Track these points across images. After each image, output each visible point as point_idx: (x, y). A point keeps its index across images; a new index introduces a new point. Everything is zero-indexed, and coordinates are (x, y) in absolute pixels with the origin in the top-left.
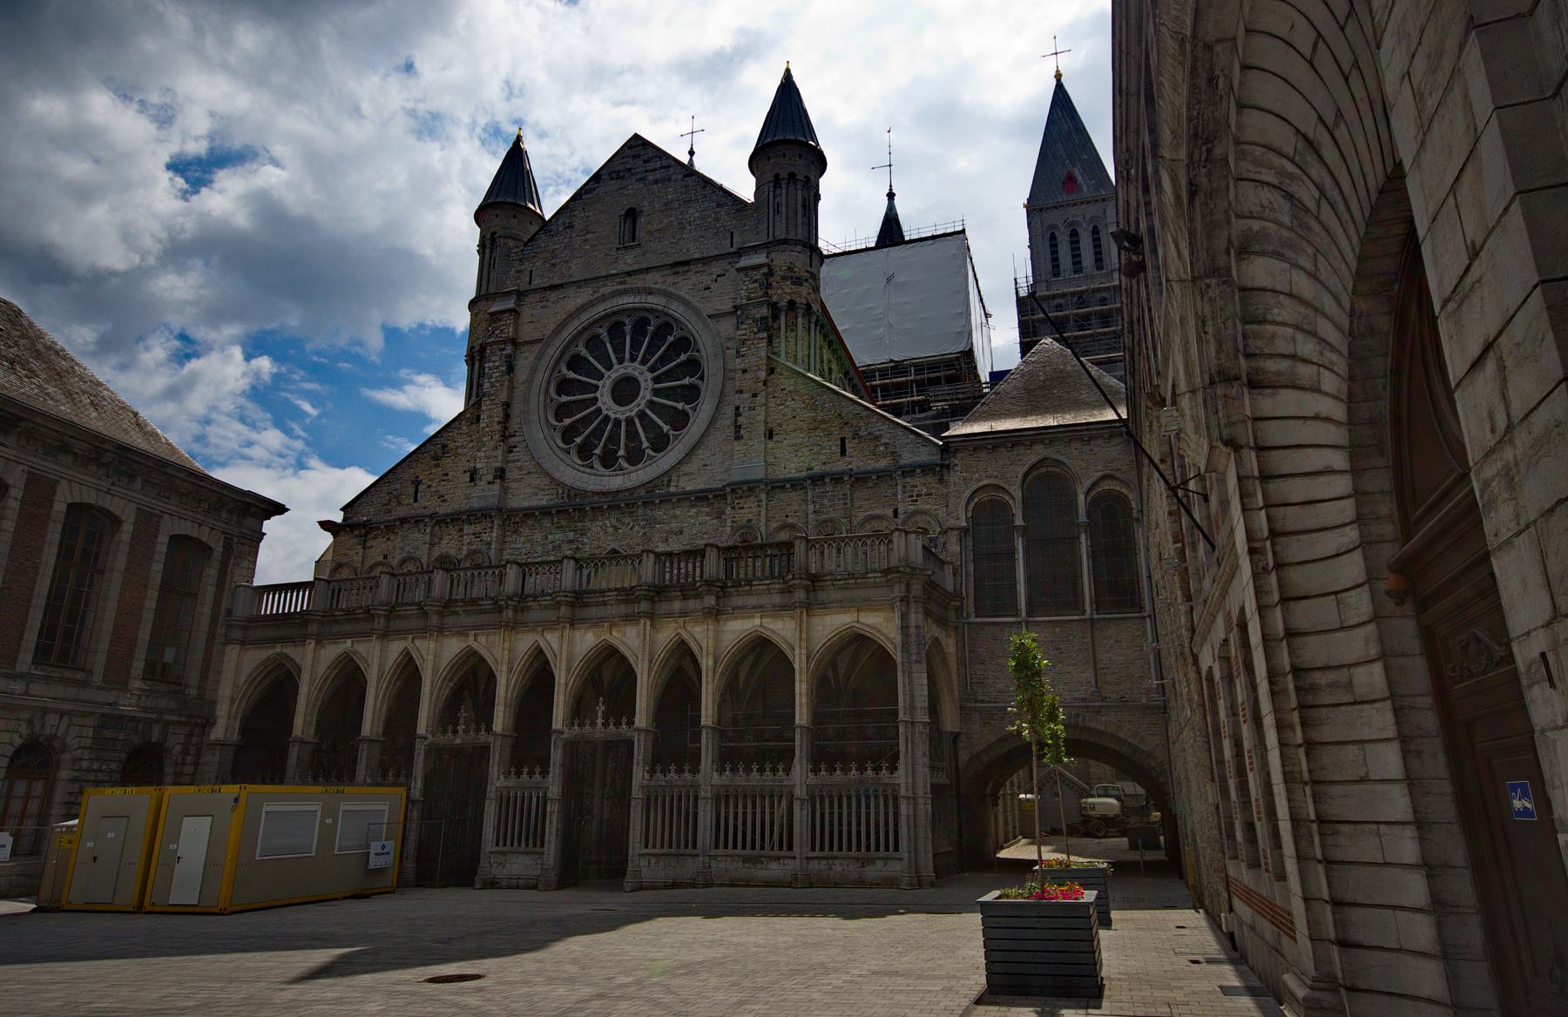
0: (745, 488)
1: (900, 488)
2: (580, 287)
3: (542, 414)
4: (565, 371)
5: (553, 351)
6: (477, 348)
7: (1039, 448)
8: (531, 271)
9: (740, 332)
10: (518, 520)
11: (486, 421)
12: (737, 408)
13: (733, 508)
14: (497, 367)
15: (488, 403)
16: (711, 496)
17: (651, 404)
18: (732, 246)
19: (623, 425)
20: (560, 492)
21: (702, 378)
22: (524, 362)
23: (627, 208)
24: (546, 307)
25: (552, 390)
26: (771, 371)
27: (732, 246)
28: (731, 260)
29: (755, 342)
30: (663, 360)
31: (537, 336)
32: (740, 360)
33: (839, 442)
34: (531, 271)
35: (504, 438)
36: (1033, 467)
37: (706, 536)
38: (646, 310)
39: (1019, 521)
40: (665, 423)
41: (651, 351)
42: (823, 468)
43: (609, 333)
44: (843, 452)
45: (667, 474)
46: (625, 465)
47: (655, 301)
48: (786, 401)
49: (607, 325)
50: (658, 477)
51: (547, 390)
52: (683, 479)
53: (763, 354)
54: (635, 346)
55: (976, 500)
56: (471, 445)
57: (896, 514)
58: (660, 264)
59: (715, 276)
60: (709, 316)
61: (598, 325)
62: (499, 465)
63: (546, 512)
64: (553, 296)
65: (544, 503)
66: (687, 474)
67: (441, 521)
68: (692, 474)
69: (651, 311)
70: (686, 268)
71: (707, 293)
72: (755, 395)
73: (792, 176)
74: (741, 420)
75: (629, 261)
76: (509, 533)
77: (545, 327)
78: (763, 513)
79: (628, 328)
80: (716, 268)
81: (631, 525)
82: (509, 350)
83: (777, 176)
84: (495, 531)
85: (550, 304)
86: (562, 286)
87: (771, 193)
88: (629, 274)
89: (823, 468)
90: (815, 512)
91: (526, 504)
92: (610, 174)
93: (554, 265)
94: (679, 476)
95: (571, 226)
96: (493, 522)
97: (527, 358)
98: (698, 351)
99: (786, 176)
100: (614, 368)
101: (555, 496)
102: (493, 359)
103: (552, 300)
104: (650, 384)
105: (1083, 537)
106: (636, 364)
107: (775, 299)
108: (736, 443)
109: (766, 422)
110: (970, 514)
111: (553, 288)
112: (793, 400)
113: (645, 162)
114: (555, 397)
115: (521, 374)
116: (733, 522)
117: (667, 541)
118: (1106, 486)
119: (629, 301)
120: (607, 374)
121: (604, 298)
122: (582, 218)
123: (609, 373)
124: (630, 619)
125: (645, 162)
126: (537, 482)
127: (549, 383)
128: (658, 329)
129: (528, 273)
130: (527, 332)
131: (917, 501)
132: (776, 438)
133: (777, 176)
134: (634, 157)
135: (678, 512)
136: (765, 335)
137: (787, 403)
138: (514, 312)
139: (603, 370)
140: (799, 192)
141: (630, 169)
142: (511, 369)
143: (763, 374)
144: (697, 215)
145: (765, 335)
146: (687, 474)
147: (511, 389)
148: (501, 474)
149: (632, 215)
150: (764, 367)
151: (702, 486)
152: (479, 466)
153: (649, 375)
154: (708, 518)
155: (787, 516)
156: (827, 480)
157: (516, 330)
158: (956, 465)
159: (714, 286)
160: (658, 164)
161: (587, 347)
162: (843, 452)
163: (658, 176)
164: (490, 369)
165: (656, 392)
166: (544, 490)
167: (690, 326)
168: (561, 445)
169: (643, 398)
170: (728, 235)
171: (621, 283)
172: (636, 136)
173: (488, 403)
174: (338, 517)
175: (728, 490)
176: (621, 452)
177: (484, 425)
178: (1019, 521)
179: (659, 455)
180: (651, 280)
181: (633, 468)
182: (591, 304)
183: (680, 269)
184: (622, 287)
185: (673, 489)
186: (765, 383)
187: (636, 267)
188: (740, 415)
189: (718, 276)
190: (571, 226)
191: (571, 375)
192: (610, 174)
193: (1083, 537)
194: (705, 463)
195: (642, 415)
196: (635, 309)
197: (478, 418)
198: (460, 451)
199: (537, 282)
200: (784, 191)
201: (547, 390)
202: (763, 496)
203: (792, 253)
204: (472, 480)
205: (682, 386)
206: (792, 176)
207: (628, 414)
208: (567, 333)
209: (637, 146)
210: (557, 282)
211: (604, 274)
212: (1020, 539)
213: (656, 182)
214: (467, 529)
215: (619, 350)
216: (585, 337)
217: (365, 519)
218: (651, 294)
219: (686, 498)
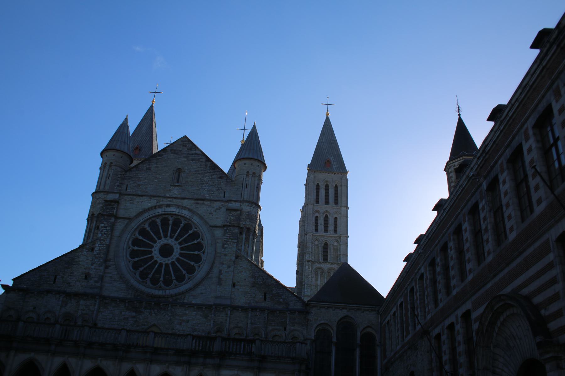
0: (222, 308)
1: (288, 319)
2: (151, 199)
3: (125, 254)
4: (137, 235)
5: (134, 225)
6: (96, 215)
7: (345, 311)
8: (127, 186)
9: (225, 237)
10: (107, 301)
11: (98, 252)
12: (220, 271)
13: (215, 315)
14: (106, 227)
15: (99, 243)
16: (204, 308)
17: (178, 260)
18: (224, 197)
19: (164, 266)
21: (204, 253)
22: (120, 226)
23: (178, 167)
25: (130, 243)
26: (237, 257)
27: (224, 197)
28: (223, 203)
29: (232, 243)
30: (186, 241)
31: (127, 216)
32: (223, 250)
33: (264, 294)
34: (127, 186)
35: (106, 260)
36: (342, 319)
37: (199, 325)
38: (181, 216)
39: (334, 340)
40: (184, 270)
41: (180, 235)
42: (256, 304)
43: (161, 222)
44: (265, 299)
45: (183, 293)
46: (163, 285)
47: (186, 213)
48: (242, 272)
49: (160, 218)
51: (128, 242)
53: (234, 249)
54: (174, 231)
55: (318, 329)
56: (87, 261)
57: (285, 329)
58: (190, 197)
59: (215, 209)
62: (101, 274)
63: (123, 300)
64: (137, 199)
65: (121, 296)
67: (70, 295)
69: (183, 217)
70: (202, 202)
72: (229, 267)
73: (254, 173)
74: (221, 276)
75: (176, 192)
76: (102, 307)
78: (228, 320)
79: (171, 222)
80: (217, 205)
81: (164, 314)
82: (113, 220)
83: (248, 172)
84: (97, 306)
86: (142, 196)
87: (244, 179)
88: (175, 198)
89: (256, 304)
90: (251, 323)
91: (112, 295)
92: (171, 150)
93: (139, 185)
95: (149, 169)
96: (96, 301)
98: (203, 240)
99: (252, 173)
102: (105, 222)
104: (179, 251)
105: (358, 350)
106: (173, 240)
107: (242, 226)
108: (218, 286)
109: (233, 280)
110: (315, 334)
111: (137, 195)
112: (245, 272)
113: (188, 149)
114: (131, 246)
115: (117, 233)
116: (214, 322)
117: (181, 324)
118: (369, 330)
119: (173, 210)
120: (158, 241)
121: (161, 206)
122: (156, 167)
123: (159, 241)
124: (178, 363)
125: (188, 149)
127: (129, 239)
128: (185, 225)
129: (125, 185)
130: (122, 213)
131: (295, 325)
132: (236, 287)
133: (248, 172)
134: (183, 146)
135: (187, 312)
136: (236, 241)
137: (243, 273)
138: (117, 202)
139: (156, 239)
140: (256, 181)
141: (181, 151)
142: (112, 230)
143: (233, 258)
144: (209, 179)
145: (236, 241)
147: (111, 239)
148: (101, 278)
149: (179, 171)
150: (234, 255)
151: (199, 302)
152: (91, 272)
153: (179, 247)
154: (201, 317)
155: (238, 323)
156: (258, 310)
157: (117, 211)
158: (312, 313)
160: (194, 152)
161: (149, 225)
162: (265, 299)
163: (194, 157)
164: (102, 227)
165: (181, 254)
168: (132, 270)
169: (175, 256)
170: (223, 192)
171: (171, 201)
172: (185, 137)
173: (99, 243)
174: (10, 284)
175: (214, 307)
176: (162, 279)
177: (95, 253)
178: (334, 340)
180: (186, 203)
181: (167, 288)
182: (155, 207)
183: (199, 202)
185: (185, 301)
186: (234, 262)
187: (179, 196)
188: (222, 275)
189: (217, 209)
190: (149, 169)
191: (141, 238)
192: (171, 150)
193: (358, 350)
195: (173, 263)
196: (175, 215)
197: (93, 249)
198: (80, 263)
199: (129, 191)
200: (250, 179)
201: (128, 242)
202: (229, 312)
203: (251, 208)
204: (86, 278)
205: (193, 254)
206: (254, 173)
207: (167, 262)
208: (142, 219)
209: (186, 141)
210: (140, 193)
211: (163, 195)
212: (334, 347)
213: (193, 160)
214: (82, 302)
215: (165, 231)
216: (149, 221)
217: (25, 287)
218: (184, 209)
219: (191, 305)
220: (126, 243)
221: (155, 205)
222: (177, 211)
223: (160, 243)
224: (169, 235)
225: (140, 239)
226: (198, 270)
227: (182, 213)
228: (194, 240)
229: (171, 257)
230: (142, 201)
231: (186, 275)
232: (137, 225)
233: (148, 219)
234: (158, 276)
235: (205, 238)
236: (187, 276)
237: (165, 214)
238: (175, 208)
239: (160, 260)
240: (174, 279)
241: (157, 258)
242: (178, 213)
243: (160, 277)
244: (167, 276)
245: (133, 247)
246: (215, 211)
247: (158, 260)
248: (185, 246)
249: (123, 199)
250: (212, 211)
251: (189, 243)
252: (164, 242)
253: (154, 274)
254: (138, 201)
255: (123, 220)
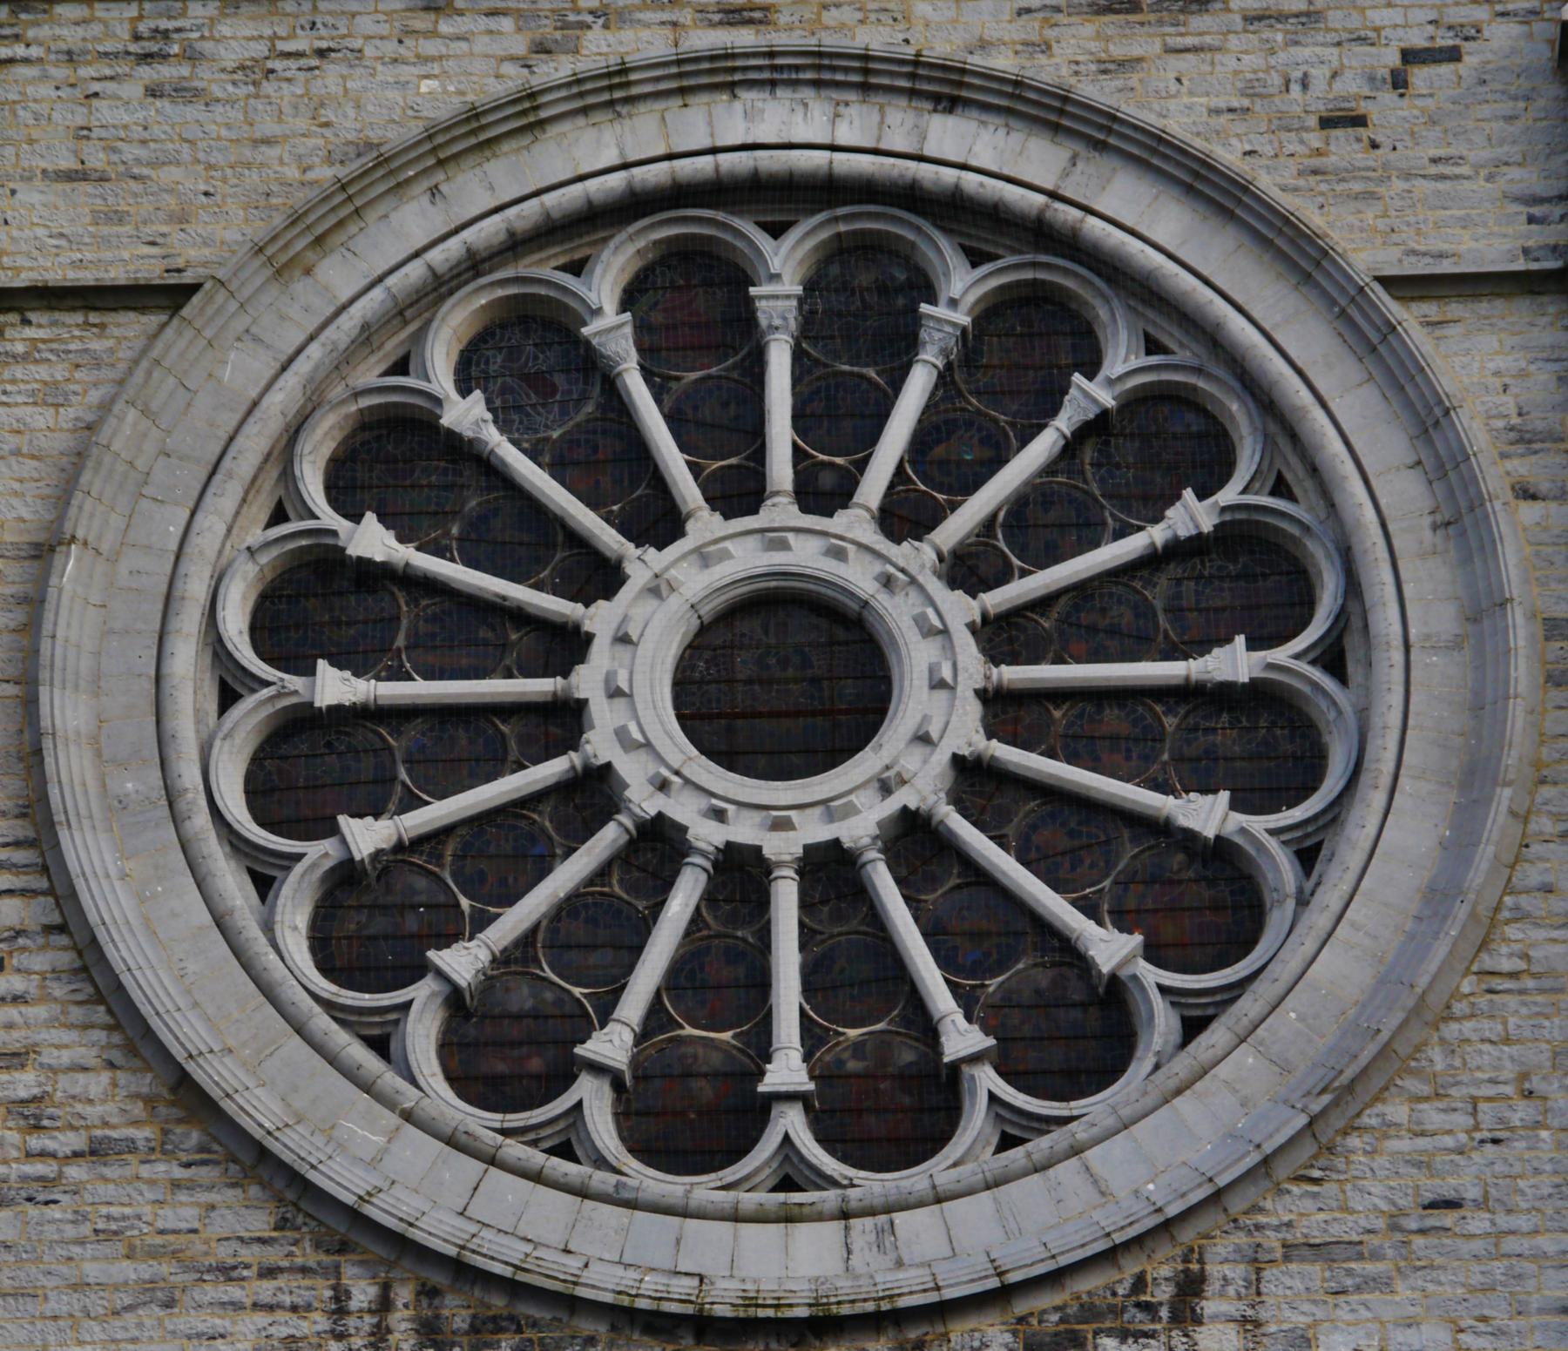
19: (786, 897)
20: (362, 1293)
21: (1332, 657)
24: (183, 92)
38: (911, 197)
50: (1110, 1256)
52: (1284, 1282)
59: (1392, 58)
60: (1386, 282)
61: (563, 252)
66: (1290, 1251)
68: (1356, 1250)
71: (1344, 147)
77: (181, 218)
85: (205, 76)
94: (1257, 1262)
97: (49, 395)
98: (1281, 488)
100: (840, 522)
101: (321, 1322)
103: (231, 55)
126: (183, 1213)
139: (608, 537)
146: (1317, 1250)
159: (1386, 110)
166: (227, 1272)
167: (1237, 326)
179: (1095, 1108)
184: (744, 38)
189: (1410, 56)
194: (1434, 1187)
218: (949, 103)
220: (189, 621)
221: (514, 79)
222: (844, 136)
223: (656, 589)
224: (781, 469)
225: (364, 564)
226: (1303, 901)
227: (930, 150)
228: (1155, 507)
229: (864, 765)
230: (322, 53)
231: (1151, 975)
232: (303, 366)
233: (440, 288)
234: (727, 1036)
235: (1335, 445)
236: (1164, 990)
237: (679, 195)
238: (807, 93)
239: (719, 815)
240: (975, 1058)
241: (663, 786)
242: (864, 164)
243: (761, 1048)
244: (853, 1033)
245: (295, 682)
246: (1399, 82)
247: (683, 809)
248: (1043, 603)
249: (34, 52)
250: (1350, 85)
251: (1095, 544)
252: (723, 572)
253: (656, 1018)
254: (261, 49)
255: (78, 318)
